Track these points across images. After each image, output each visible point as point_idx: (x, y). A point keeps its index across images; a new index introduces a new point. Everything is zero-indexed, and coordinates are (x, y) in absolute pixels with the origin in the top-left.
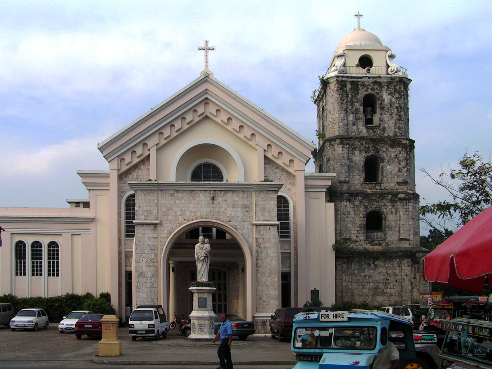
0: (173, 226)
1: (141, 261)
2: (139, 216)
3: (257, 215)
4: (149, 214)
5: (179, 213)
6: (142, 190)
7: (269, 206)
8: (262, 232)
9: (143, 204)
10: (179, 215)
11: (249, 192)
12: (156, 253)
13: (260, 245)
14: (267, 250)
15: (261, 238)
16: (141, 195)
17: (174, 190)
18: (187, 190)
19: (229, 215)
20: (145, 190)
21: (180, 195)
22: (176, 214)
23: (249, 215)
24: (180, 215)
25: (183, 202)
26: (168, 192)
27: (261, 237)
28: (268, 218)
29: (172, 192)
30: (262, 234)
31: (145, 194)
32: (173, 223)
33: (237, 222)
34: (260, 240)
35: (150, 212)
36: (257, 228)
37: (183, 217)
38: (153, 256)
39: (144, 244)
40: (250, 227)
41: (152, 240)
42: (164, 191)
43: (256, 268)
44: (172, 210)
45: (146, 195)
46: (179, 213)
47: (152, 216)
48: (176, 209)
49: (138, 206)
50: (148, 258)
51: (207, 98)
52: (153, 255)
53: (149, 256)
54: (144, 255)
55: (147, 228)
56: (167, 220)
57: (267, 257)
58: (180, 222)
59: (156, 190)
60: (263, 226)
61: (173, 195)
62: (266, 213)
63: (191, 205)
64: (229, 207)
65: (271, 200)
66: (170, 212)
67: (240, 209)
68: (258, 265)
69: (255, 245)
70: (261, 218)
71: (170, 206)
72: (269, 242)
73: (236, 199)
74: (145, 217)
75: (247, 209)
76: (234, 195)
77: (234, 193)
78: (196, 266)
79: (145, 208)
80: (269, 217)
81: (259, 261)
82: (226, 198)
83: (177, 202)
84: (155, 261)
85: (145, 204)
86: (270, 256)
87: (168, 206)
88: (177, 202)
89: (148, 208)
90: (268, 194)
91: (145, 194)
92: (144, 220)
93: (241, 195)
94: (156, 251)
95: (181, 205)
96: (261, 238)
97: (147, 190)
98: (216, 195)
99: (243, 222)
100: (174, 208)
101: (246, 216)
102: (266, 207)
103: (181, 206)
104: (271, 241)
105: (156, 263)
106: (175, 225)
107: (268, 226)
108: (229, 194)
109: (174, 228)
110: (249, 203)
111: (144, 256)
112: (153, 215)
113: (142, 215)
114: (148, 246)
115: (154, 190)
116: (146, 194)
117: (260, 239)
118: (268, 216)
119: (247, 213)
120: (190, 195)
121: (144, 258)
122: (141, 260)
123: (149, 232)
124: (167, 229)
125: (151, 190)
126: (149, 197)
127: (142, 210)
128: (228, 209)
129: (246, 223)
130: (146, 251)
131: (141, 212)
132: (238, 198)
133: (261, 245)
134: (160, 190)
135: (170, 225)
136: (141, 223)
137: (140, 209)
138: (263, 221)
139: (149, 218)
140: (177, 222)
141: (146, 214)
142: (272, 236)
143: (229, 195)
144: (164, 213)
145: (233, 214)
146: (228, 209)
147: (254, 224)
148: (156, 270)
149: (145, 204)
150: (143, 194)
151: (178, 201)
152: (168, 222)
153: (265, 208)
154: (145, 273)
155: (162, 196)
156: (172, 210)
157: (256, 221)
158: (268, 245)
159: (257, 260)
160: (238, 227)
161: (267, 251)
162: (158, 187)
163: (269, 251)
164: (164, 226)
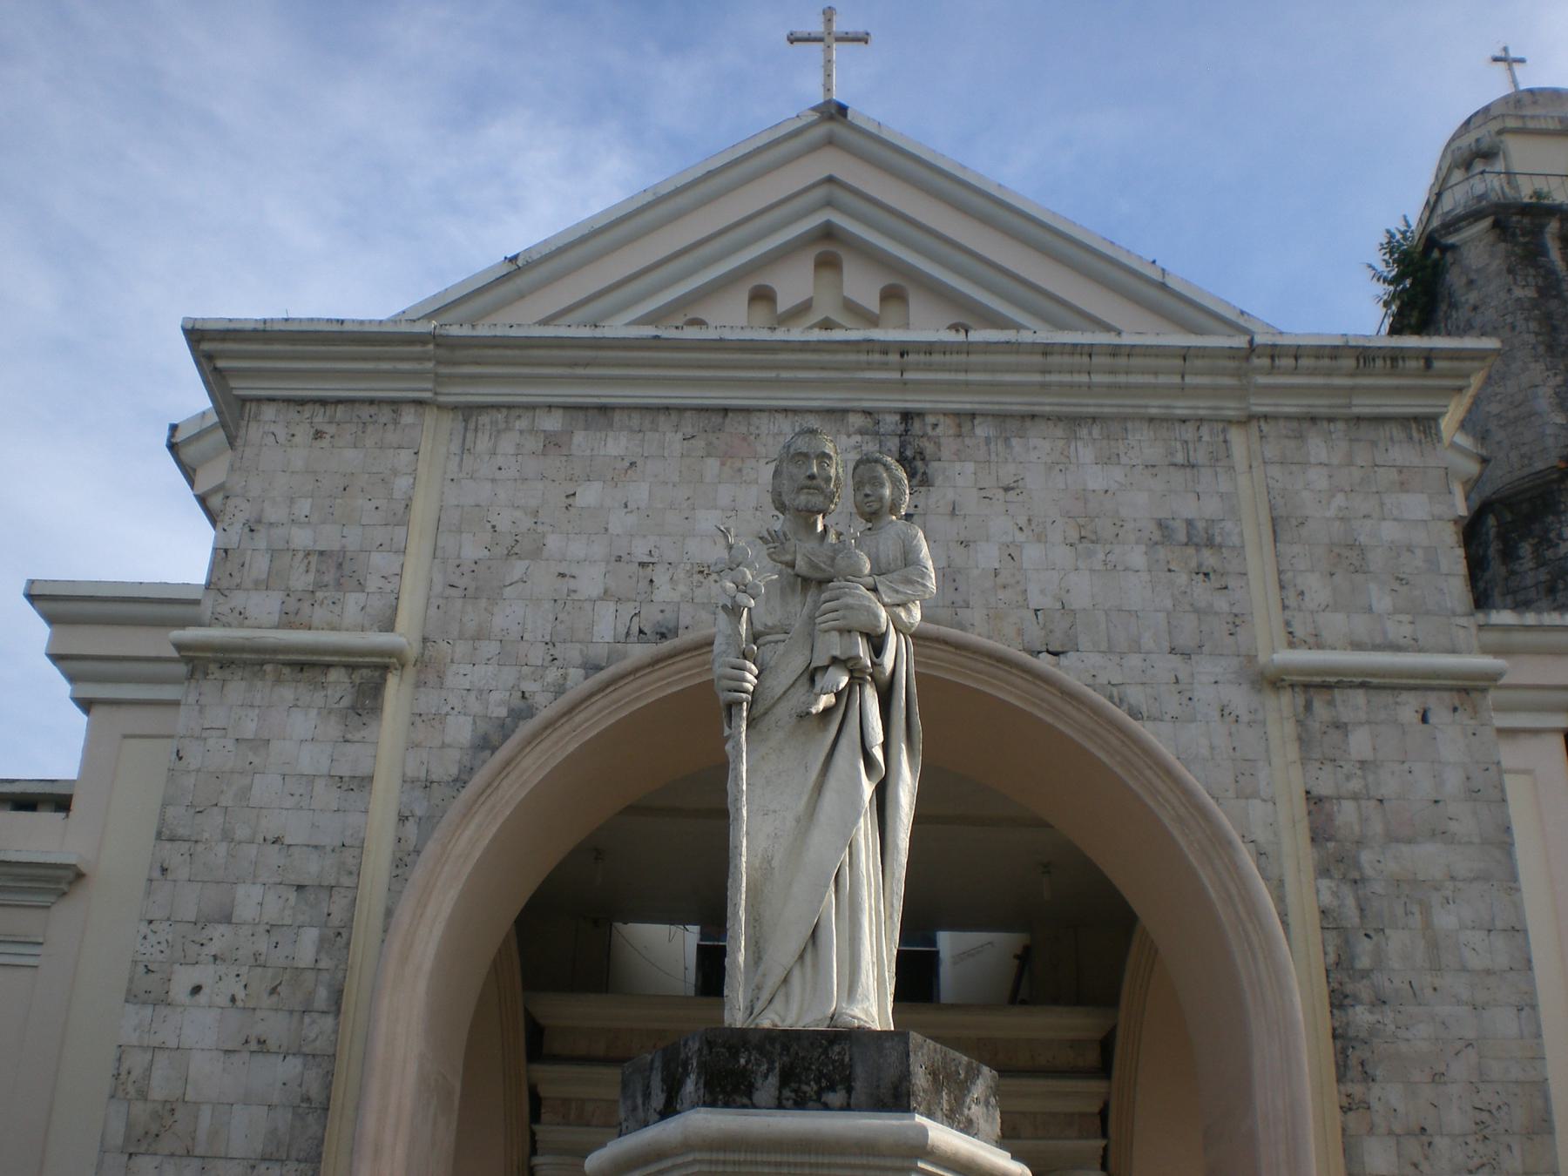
0: (528, 686)
1: (179, 991)
2: (238, 599)
3: (1292, 601)
4: (329, 578)
5: (590, 582)
6: (302, 402)
7: (1390, 531)
8: (1360, 743)
9: (292, 500)
10: (596, 591)
11: (1205, 430)
12: (336, 920)
13: (1357, 865)
14: (1426, 910)
15: (1355, 797)
16: (282, 438)
17: (566, 408)
18: (681, 410)
19: (1047, 602)
20: (323, 402)
21: (616, 444)
22: (572, 584)
23: (1221, 603)
24: (606, 594)
25: (640, 492)
26: (522, 424)
27: (1355, 785)
28: (1398, 630)
29: (552, 423)
30: (1363, 763)
31: (318, 435)
32: (537, 655)
33: (1122, 655)
34: (1346, 814)
35: (340, 565)
36: (1308, 707)
37: (628, 609)
38: (306, 947)
39: (241, 833)
40: (1240, 698)
41: (326, 796)
42: (485, 419)
43: (1341, 1078)
44: (537, 552)
45: (325, 443)
46: (590, 582)
47: (353, 601)
48: (577, 548)
49: (241, 518)
50: (257, 961)
51: (828, 233)
52: (310, 936)
53: (262, 945)
54: (220, 937)
55: (287, 693)
56: (477, 638)
57: (1436, 968)
58: (599, 652)
59: (419, 403)
60: (1359, 697)
61: (553, 443)
62: (1373, 586)
63: (708, 520)
64: (1041, 538)
65: (1403, 487)
66: (518, 568)
67: (1137, 557)
68: (1354, 1057)
69: (1296, 855)
70: (1335, 624)
71: (527, 523)
72: (1439, 834)
73: (1096, 479)
74: (292, 604)
75: (1209, 559)
76: (1086, 453)
77: (1084, 432)
78: (719, 816)
79: (302, 538)
80: (1406, 618)
81: (1362, 1016)
82: (1008, 473)
83: (589, 495)
84: (322, 994)
85: (304, 507)
86: (1464, 969)
87: (503, 524)
88: (589, 495)
89: (329, 538)
90: (1374, 443)
91: (318, 435)
92: (278, 626)
93: (1144, 445)
94: (338, 906)
95: (618, 522)
96: (1355, 797)
97: (339, 402)
98: (929, 448)
99: (1176, 660)
100: (553, 542)
101: (1197, 611)
102: (1362, 539)
103: (615, 528)
104: (1453, 827)
105: (329, 1021)
106: (552, 675)
107: (1405, 696)
108: (1033, 442)
109: (540, 699)
110: (1211, 507)
111: (213, 948)
112: (361, 586)
113: (264, 585)
114: (273, 854)
115: (395, 404)
116: (331, 429)
117: (1348, 807)
118: (1396, 611)
119: (1201, 592)
120: (700, 443)
121: (222, 968)
122: (184, 978)
123: (302, 723)
124: (475, 706)
125: (372, 402)
126: (350, 453)
127: (274, 553)
128: (1032, 553)
129: (1206, 668)
130: (248, 901)
131: (260, 565)
132: (1117, 474)
133: (1366, 857)
134: (455, 408)
135: (509, 675)
136: (242, 649)
137: (261, 541)
138: (1357, 646)
139: (319, 614)
140: (573, 653)
141: (301, 580)
142: (1453, 781)
143: (1040, 446)
144: (462, 583)
145: (1082, 589)
146: (1032, 553)
147: (1274, 682)
148: (314, 1089)
149: (304, 507)
150: (303, 433)
151: (597, 485)
152: (490, 648)
153: (1362, 550)
154: (206, 1114)
155: (464, 450)
156: (537, 552)
157: (1292, 645)
158: (1428, 858)
159: (1339, 1001)
160: (1136, 695)
161: (1428, 925)
162: (438, 378)
163: (1445, 920)
164: (450, 681)
